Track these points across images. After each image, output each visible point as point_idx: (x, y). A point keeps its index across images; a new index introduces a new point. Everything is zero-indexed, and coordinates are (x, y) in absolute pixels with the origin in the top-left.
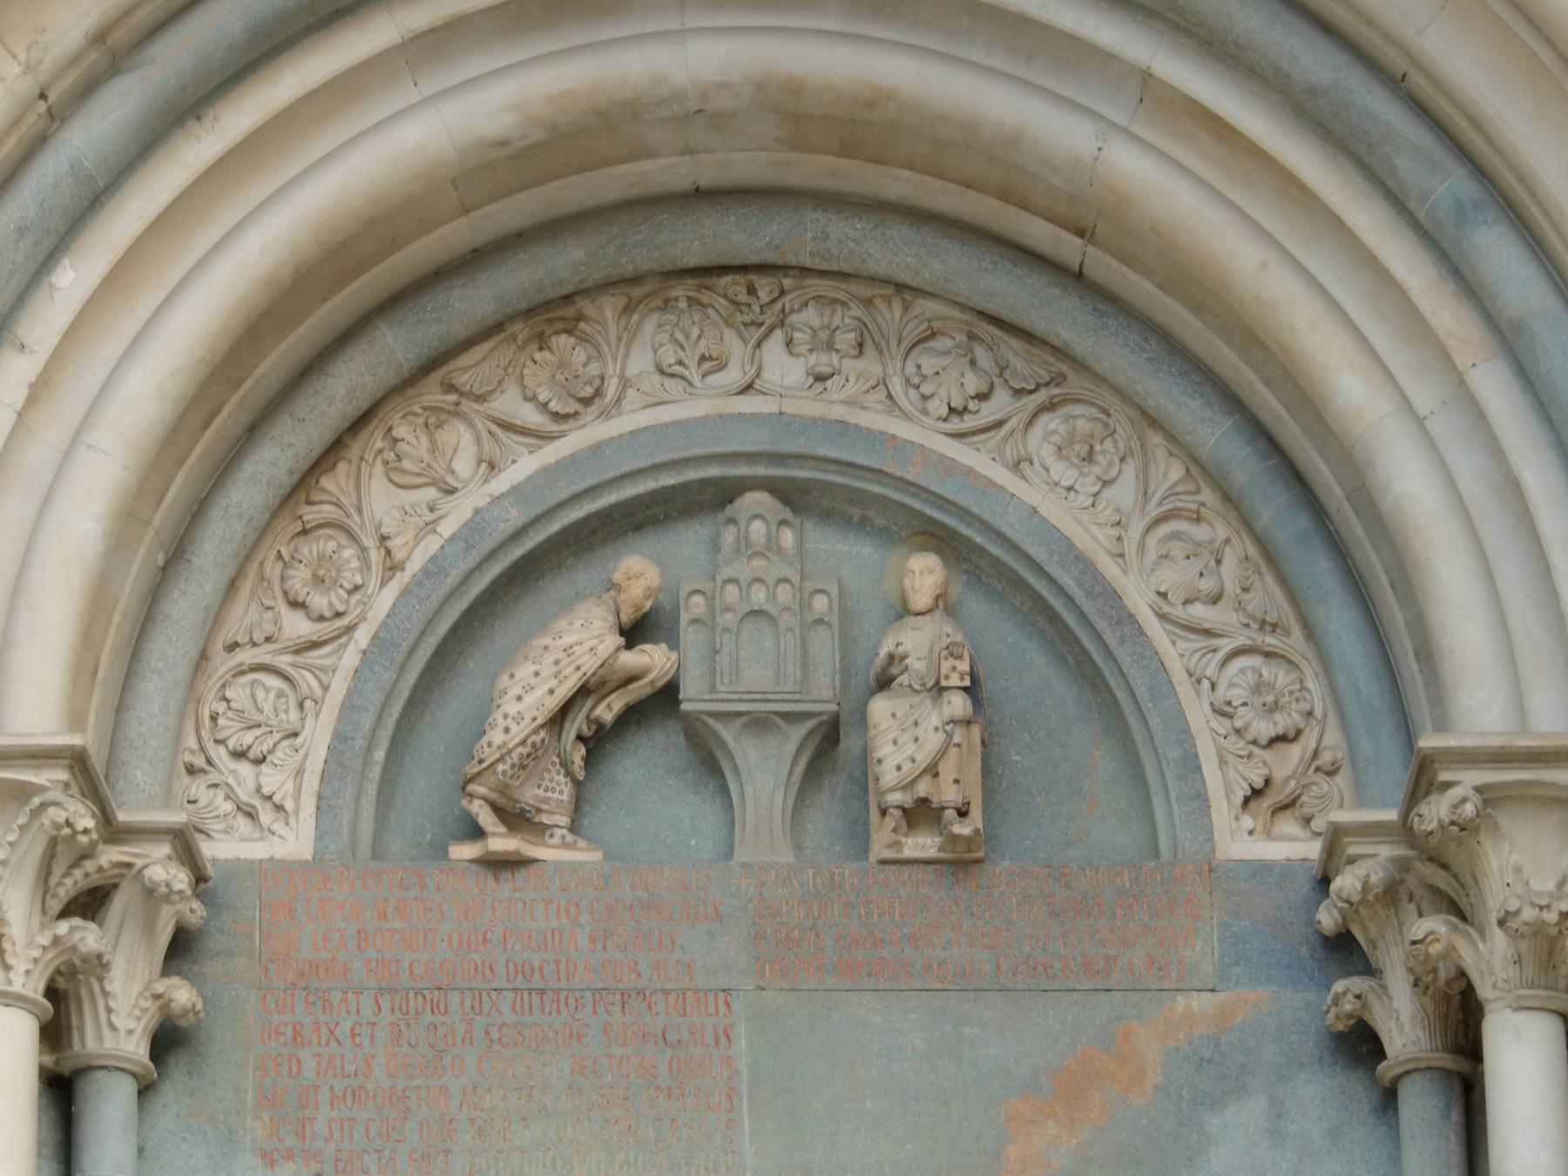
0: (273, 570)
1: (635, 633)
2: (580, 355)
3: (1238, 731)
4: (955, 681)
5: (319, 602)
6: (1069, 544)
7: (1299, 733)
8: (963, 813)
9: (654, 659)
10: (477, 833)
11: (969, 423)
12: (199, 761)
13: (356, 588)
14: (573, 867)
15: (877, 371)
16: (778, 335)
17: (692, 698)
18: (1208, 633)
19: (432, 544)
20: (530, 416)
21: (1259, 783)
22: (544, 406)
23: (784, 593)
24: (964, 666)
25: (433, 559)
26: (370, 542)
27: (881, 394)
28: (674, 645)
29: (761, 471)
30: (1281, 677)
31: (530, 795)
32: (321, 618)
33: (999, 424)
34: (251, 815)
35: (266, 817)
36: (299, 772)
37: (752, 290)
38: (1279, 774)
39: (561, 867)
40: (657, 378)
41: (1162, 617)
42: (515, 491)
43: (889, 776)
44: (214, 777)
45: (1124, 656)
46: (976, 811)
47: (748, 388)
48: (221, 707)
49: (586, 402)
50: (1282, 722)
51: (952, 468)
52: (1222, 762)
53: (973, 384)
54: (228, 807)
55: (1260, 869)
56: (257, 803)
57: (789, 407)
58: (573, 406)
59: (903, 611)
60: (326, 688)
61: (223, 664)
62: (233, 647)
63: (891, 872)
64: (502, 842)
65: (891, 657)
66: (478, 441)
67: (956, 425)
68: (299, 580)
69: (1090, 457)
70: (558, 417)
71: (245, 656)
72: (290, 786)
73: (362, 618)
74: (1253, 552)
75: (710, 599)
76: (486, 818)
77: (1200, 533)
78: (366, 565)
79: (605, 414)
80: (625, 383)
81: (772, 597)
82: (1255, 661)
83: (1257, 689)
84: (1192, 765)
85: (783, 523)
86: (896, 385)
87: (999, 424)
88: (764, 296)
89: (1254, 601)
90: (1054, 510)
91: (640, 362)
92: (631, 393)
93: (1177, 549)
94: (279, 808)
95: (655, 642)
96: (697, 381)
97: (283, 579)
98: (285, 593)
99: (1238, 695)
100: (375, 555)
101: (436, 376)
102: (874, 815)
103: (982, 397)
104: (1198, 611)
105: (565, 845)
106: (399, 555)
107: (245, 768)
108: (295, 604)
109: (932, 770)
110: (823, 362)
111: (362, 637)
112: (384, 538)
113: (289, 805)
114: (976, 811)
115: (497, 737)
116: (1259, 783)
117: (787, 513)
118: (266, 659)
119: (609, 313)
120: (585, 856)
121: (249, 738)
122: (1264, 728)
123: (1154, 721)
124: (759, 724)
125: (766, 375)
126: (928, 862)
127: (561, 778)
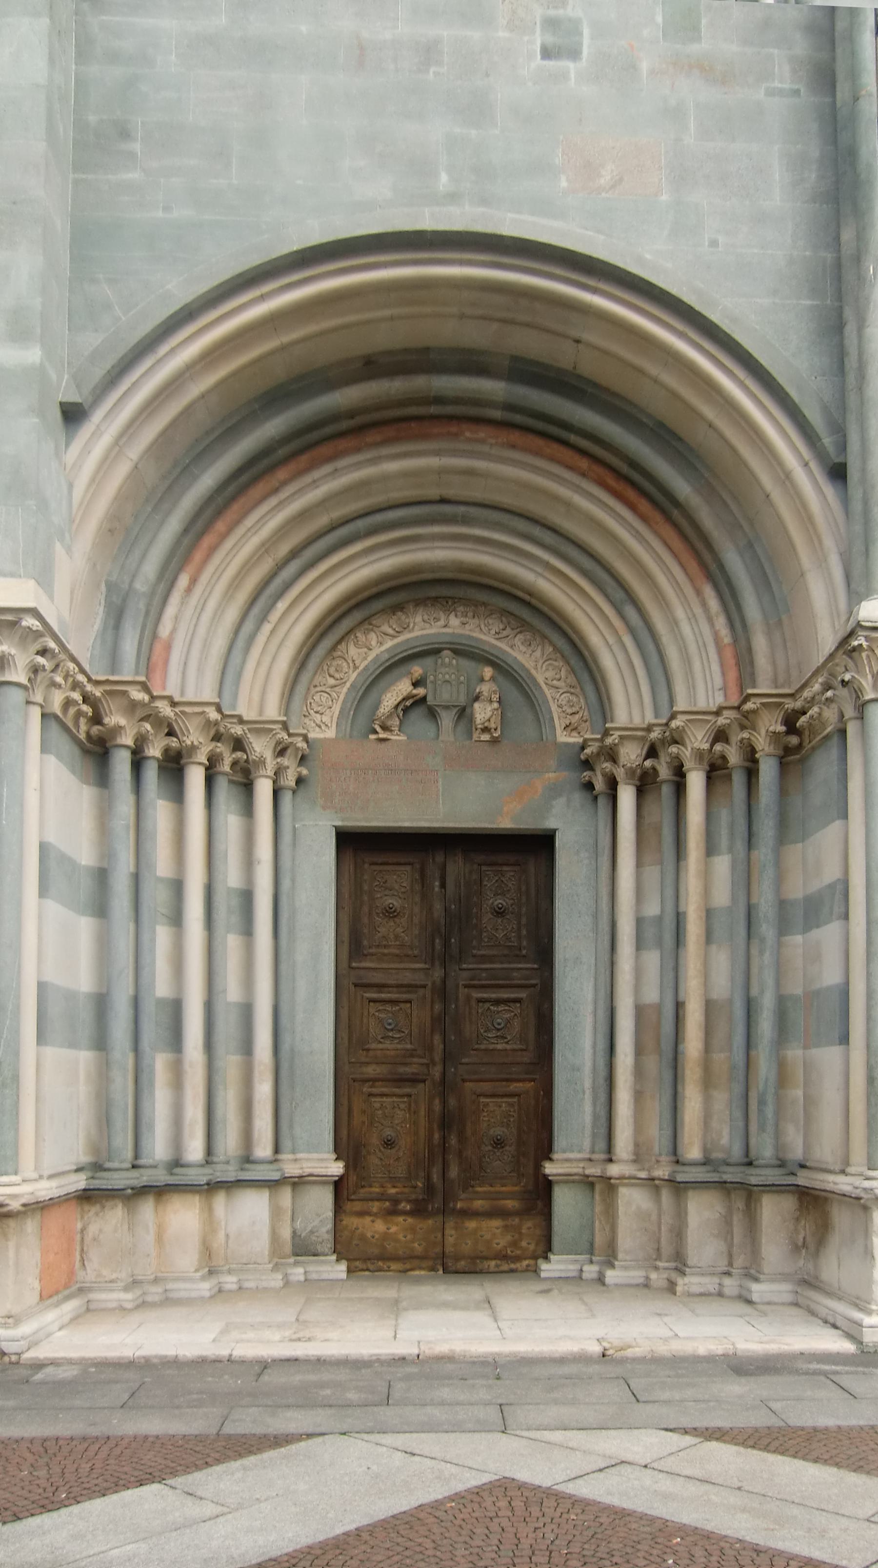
0: (325, 668)
1: (415, 684)
2: (403, 617)
3: (563, 712)
4: (495, 699)
5: (337, 676)
6: (523, 666)
7: (578, 712)
8: (496, 729)
9: (420, 691)
10: (376, 732)
11: (500, 636)
12: (307, 714)
13: (346, 673)
14: (400, 741)
15: (478, 622)
16: (453, 613)
17: (430, 700)
18: (557, 688)
19: (366, 663)
20: (390, 631)
21: (568, 724)
22: (395, 630)
23: (453, 676)
24: (498, 696)
25: (366, 666)
26: (350, 662)
27: (479, 628)
28: (426, 688)
29: (448, 646)
30: (575, 699)
31: (389, 723)
32: (337, 680)
33: (507, 636)
34: (320, 727)
35: (323, 727)
36: (332, 717)
37: (447, 602)
38: (573, 721)
39: (396, 740)
40: (423, 623)
41: (546, 684)
42: (387, 650)
43: (478, 721)
44: (310, 717)
45: (536, 693)
46: (499, 729)
47: (445, 626)
48: (312, 701)
49: (405, 628)
50: (574, 710)
51: (495, 647)
52: (559, 718)
53: (501, 626)
54: (314, 725)
55: (567, 744)
56: (322, 725)
57: (456, 631)
58: (402, 630)
59: (482, 680)
60: (338, 697)
61: (313, 690)
62: (315, 686)
63: (477, 744)
64: (382, 735)
65: (479, 693)
66: (378, 637)
67: (497, 636)
68: (332, 670)
69: (530, 645)
70: (397, 632)
71: (319, 689)
72: (329, 720)
73: (348, 680)
74: (569, 669)
75: (435, 677)
76: (378, 729)
77: (556, 664)
78: (349, 667)
79: (410, 632)
80: (414, 623)
81: (450, 677)
82: (569, 695)
83: (569, 701)
84: (552, 719)
85: (454, 658)
86: (483, 626)
87: (507, 636)
88: (450, 603)
89: (568, 681)
90: (520, 658)
91: (418, 619)
92: (416, 627)
93: (550, 668)
94: (327, 725)
95: (421, 687)
96: (433, 624)
97: (328, 670)
98: (329, 674)
99: (564, 703)
100: (351, 665)
101: (367, 622)
102: (474, 729)
103: (504, 629)
104: (555, 682)
105: (397, 735)
106: (357, 665)
107: (318, 716)
108: (331, 676)
109: (489, 720)
110: (464, 620)
111: (348, 685)
112: (353, 661)
113: (329, 725)
114: (499, 729)
115: (382, 710)
116: (568, 724)
117: (454, 656)
118: (324, 689)
119: (411, 607)
120: (403, 738)
121: (319, 708)
122: (570, 711)
123: (543, 709)
124: (447, 708)
125: (450, 622)
126: (487, 741)
127: (397, 719)
